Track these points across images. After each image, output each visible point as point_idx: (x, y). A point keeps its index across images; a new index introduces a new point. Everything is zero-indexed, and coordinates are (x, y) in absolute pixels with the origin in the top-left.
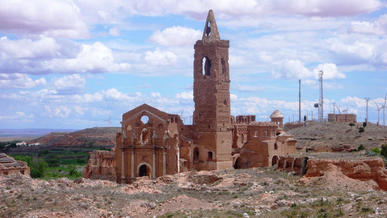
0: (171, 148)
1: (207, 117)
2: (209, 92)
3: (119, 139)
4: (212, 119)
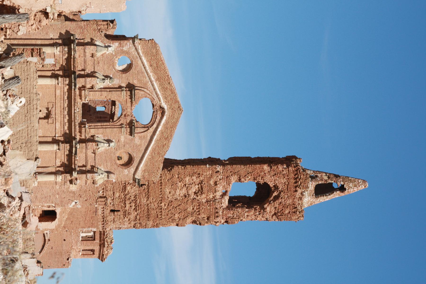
0: (74, 193)
1: (136, 203)
2: (193, 209)
3: (94, 30)
4: (132, 217)
